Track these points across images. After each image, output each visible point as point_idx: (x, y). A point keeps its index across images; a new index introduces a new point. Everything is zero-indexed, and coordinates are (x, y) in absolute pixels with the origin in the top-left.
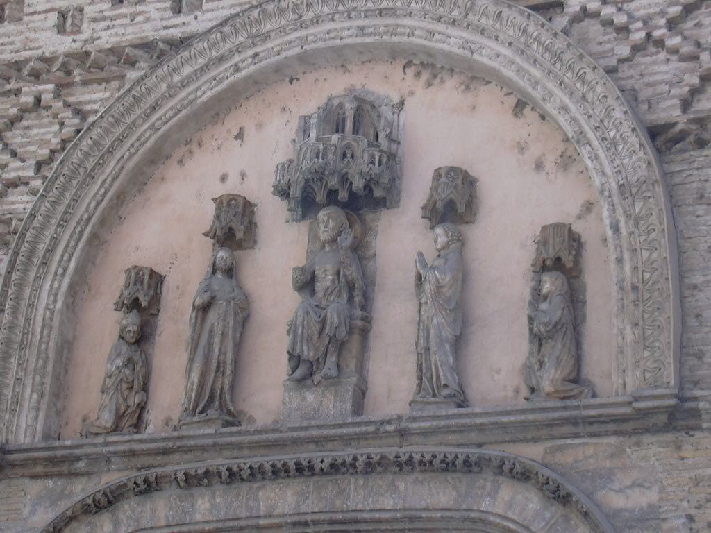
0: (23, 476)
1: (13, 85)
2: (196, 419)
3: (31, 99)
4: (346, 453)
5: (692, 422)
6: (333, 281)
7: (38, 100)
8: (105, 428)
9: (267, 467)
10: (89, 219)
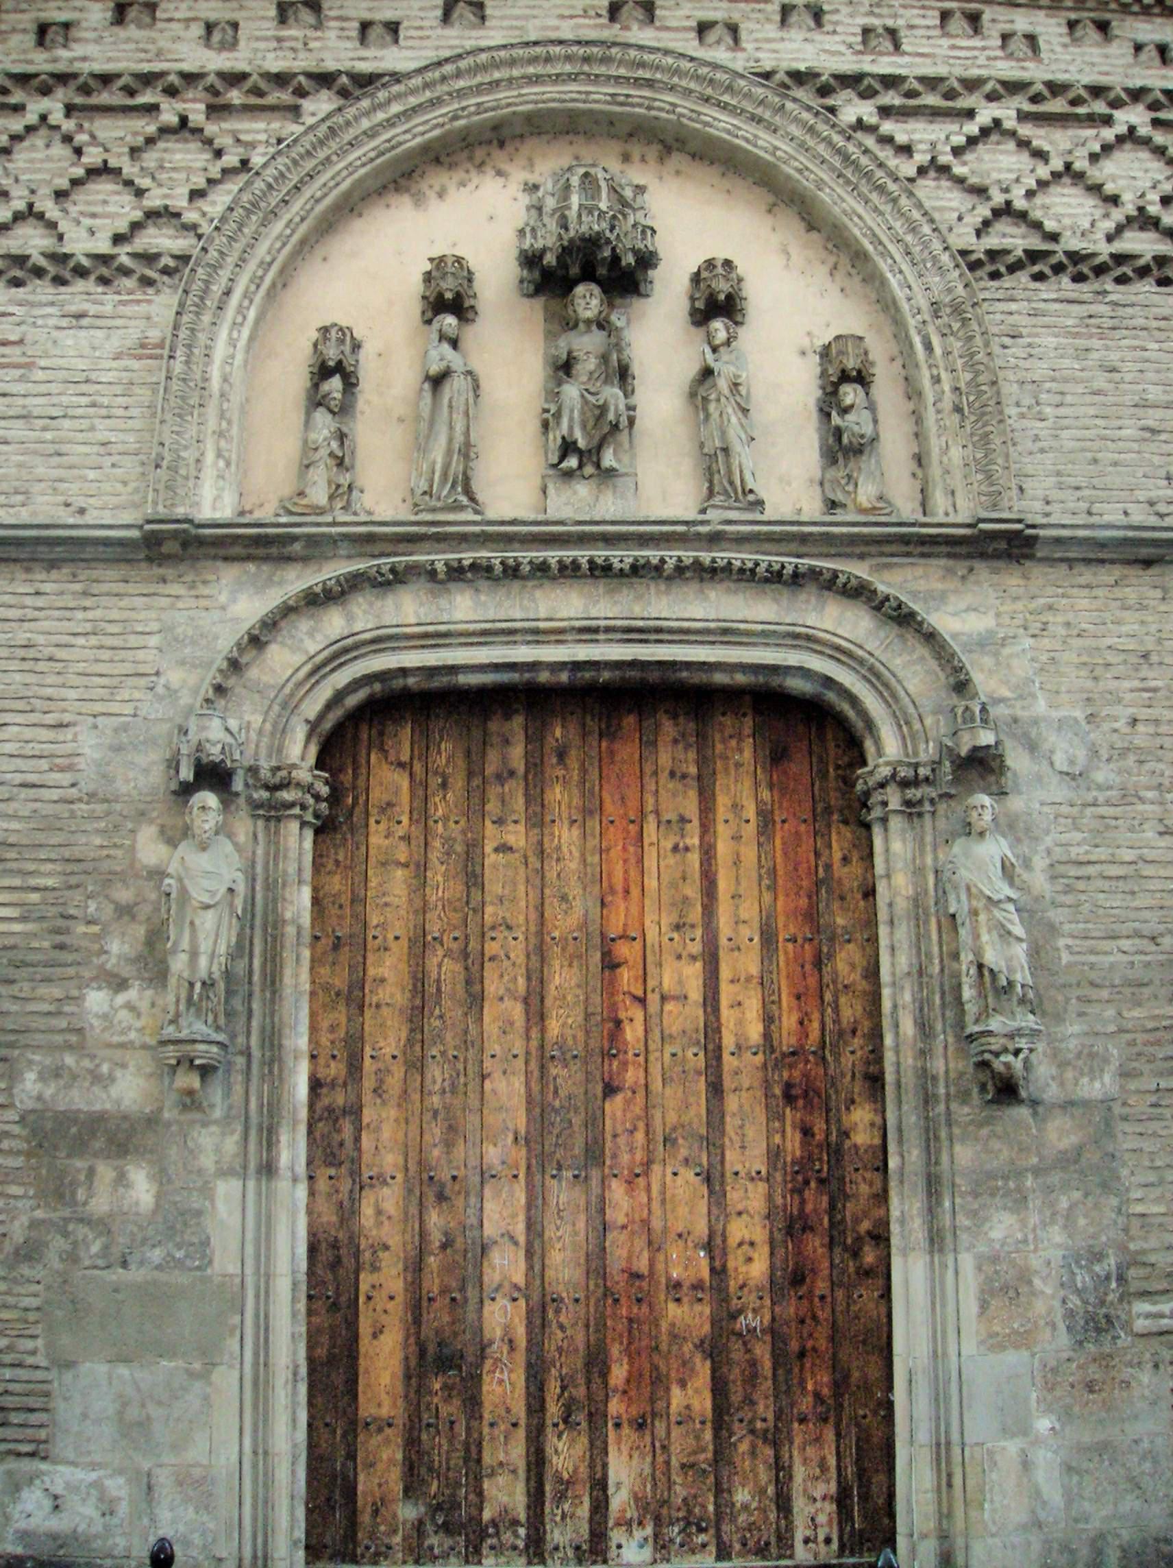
0: (215, 558)
1: (146, 98)
2: (439, 504)
3: (175, 120)
4: (652, 554)
5: (1026, 551)
6: (598, 366)
7: (184, 120)
8: (318, 507)
9: (584, 561)
10: (270, 264)
